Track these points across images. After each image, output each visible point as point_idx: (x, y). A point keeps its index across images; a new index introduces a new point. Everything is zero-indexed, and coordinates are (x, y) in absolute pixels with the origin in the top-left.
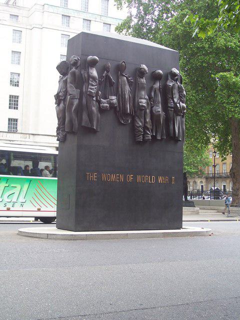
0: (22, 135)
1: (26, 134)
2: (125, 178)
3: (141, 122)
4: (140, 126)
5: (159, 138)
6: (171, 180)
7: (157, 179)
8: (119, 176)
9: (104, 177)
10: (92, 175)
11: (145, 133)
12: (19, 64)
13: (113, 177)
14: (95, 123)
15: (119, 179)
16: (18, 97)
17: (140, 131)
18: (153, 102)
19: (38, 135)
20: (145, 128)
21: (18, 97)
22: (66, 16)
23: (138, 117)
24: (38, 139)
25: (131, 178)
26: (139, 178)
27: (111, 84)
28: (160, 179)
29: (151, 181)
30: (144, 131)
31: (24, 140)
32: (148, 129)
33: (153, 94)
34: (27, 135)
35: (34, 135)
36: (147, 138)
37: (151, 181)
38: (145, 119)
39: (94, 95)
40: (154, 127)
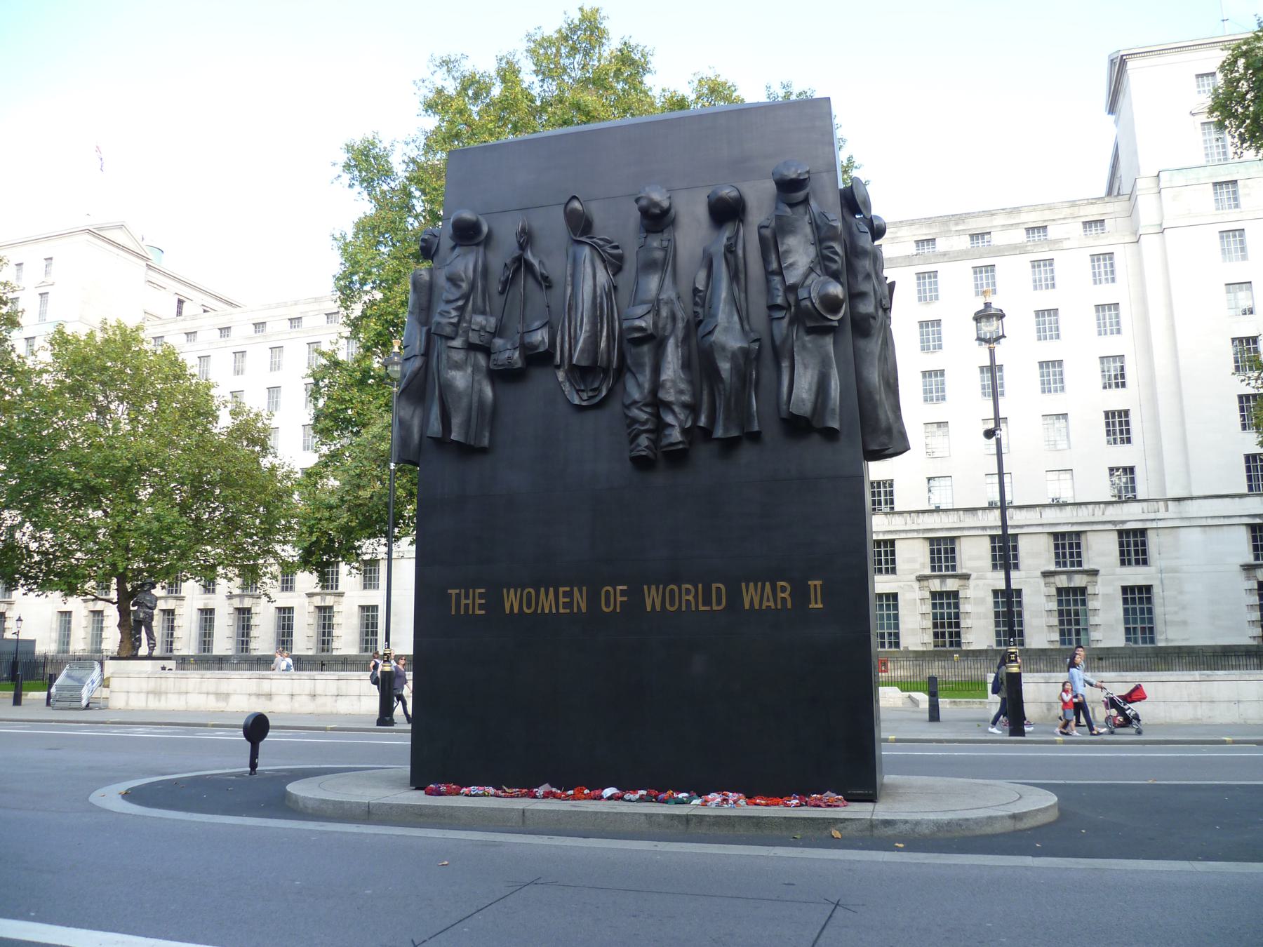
0: (1145, 504)
1: (1157, 500)
2: (593, 599)
3: (640, 386)
4: (635, 402)
5: (719, 433)
6: (801, 594)
7: (735, 597)
8: (569, 594)
9: (512, 601)
10: (467, 597)
11: (660, 427)
12: (1119, 331)
13: (547, 602)
14: (456, 422)
15: (568, 605)
16: (1126, 413)
17: (635, 421)
18: (703, 306)
19: (1192, 498)
20: (657, 404)
21: (1126, 413)
22: (1227, 183)
23: (634, 375)
24: (1193, 508)
25: (615, 596)
26: (652, 598)
27: (545, 282)
28: (751, 596)
29: (707, 602)
30: (657, 416)
31: (1152, 516)
32: (668, 406)
33: (702, 275)
34: (1161, 503)
35: (1179, 500)
36: (665, 442)
37: (707, 602)
38: (657, 370)
39: (448, 330)
40: (705, 397)
